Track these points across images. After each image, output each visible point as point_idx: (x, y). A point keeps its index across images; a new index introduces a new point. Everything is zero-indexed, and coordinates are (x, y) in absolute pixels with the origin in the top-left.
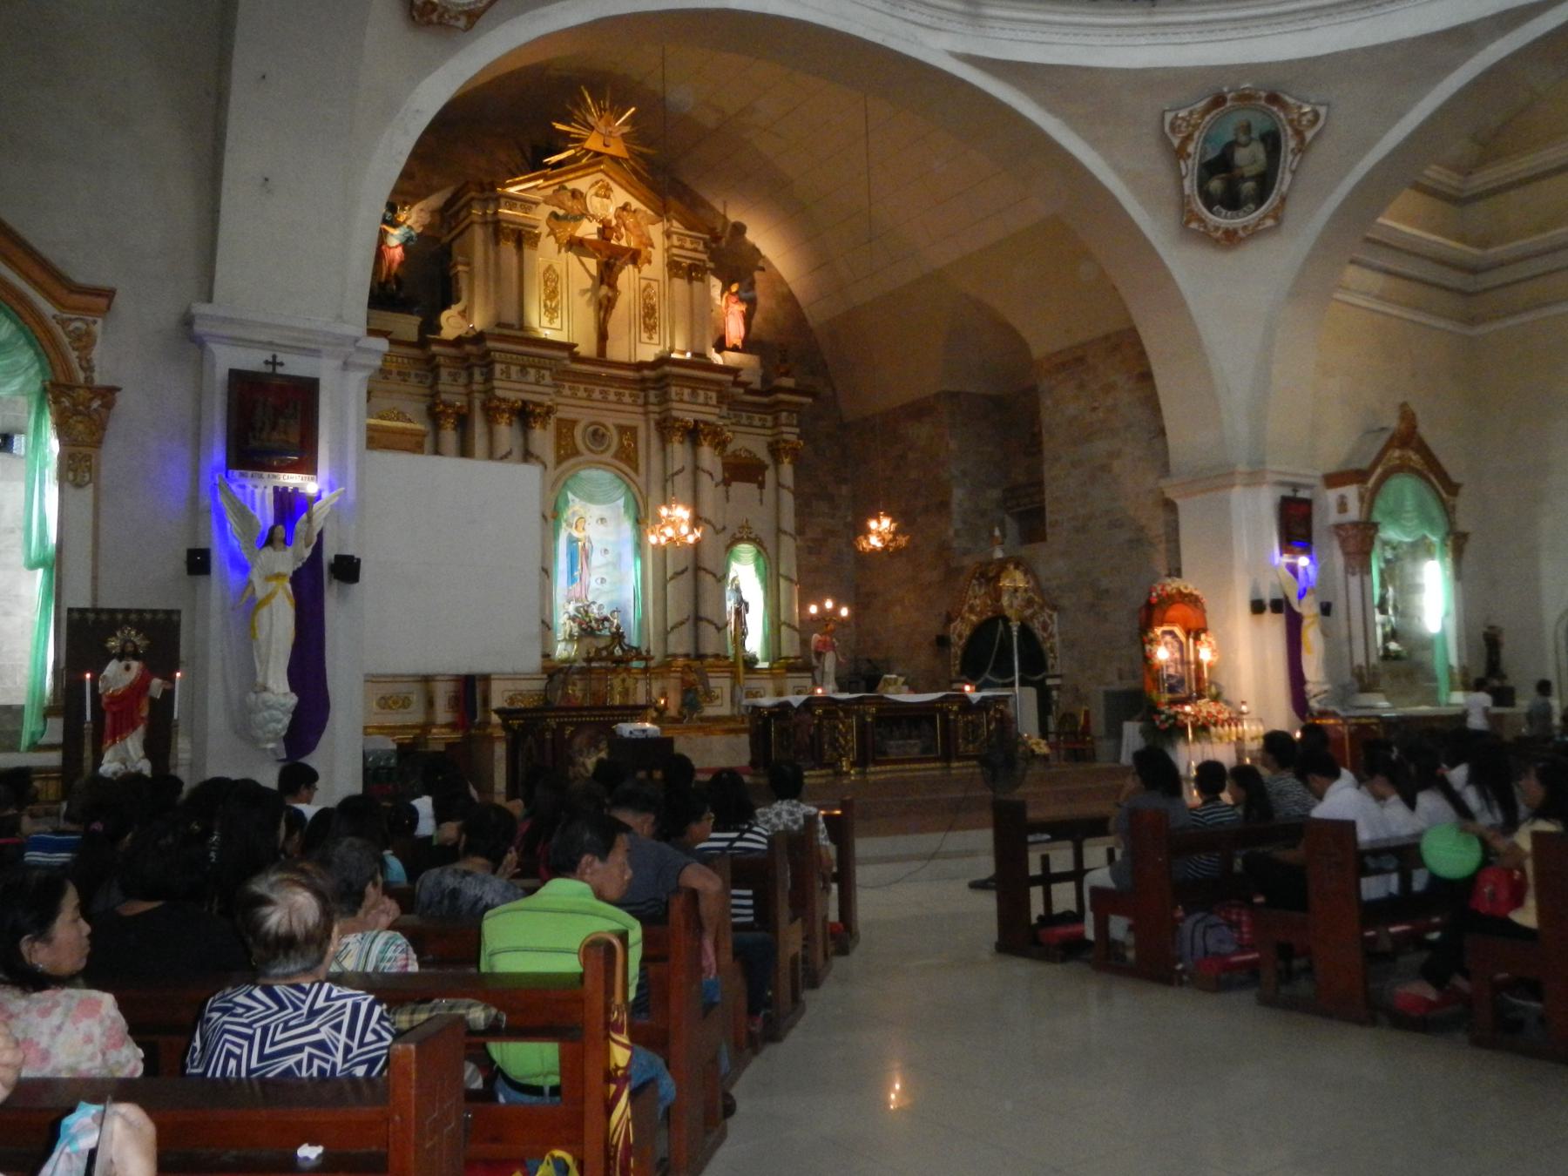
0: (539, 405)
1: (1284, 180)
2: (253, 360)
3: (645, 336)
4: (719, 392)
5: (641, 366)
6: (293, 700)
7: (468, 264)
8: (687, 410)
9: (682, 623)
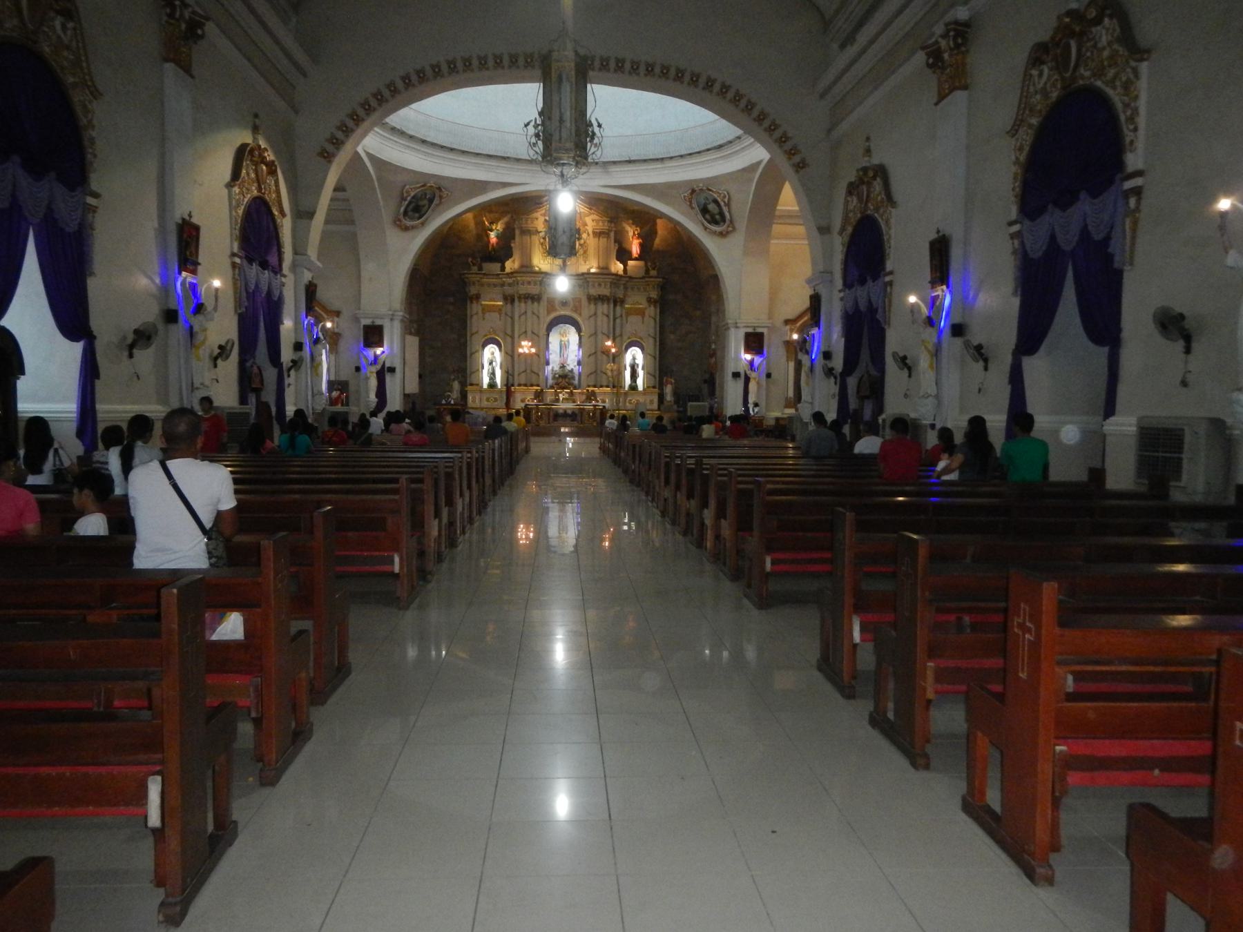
0: (536, 295)
1: (727, 214)
2: (368, 322)
3: (583, 263)
4: (611, 283)
5: (578, 275)
6: (376, 400)
7: (514, 243)
8: (594, 292)
9: (591, 374)
